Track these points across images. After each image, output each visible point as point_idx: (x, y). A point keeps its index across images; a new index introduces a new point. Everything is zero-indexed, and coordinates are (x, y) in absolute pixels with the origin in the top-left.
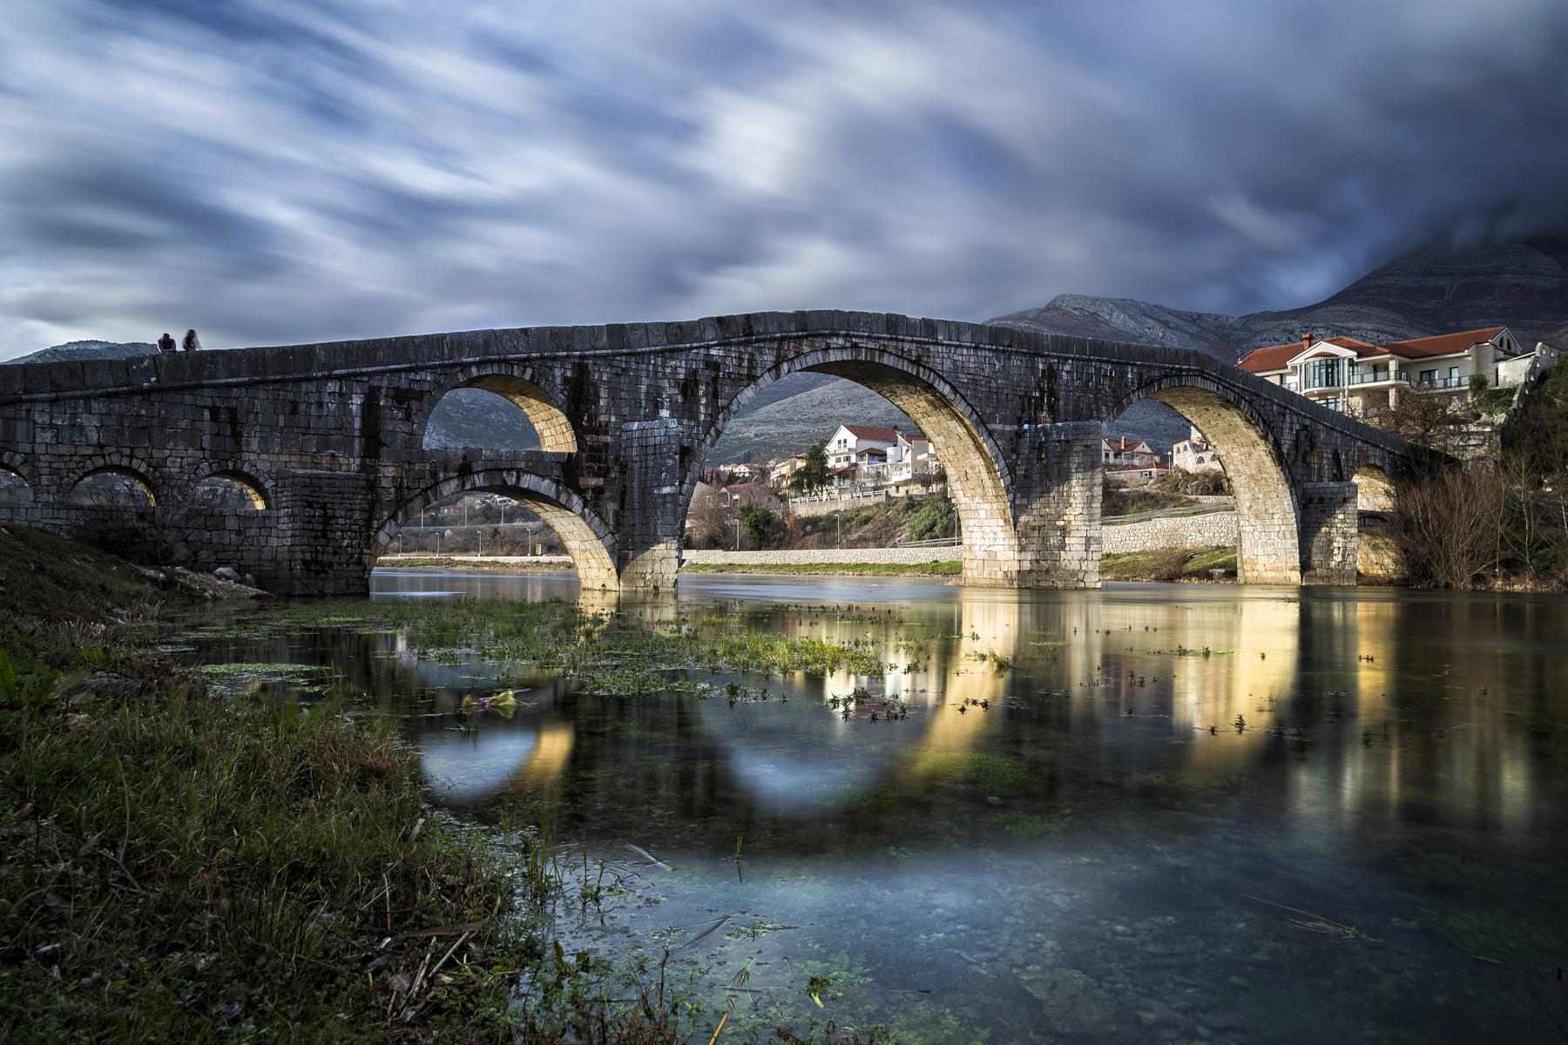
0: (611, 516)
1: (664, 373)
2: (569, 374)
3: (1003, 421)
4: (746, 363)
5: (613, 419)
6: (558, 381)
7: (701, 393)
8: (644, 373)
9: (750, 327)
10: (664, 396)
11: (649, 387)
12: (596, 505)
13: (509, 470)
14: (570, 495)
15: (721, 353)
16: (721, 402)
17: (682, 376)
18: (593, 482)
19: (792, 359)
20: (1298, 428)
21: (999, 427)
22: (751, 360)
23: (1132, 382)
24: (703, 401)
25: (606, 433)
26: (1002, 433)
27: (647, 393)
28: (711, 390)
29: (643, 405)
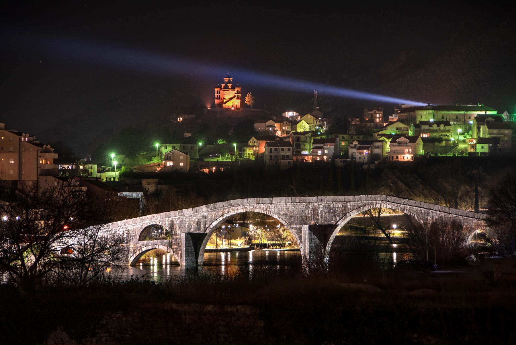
0: (179, 254)
1: (192, 220)
2: (169, 223)
3: (296, 224)
4: (213, 216)
5: (180, 232)
6: (167, 224)
7: (201, 224)
8: (187, 221)
9: (215, 207)
10: (192, 226)
11: (188, 224)
12: (176, 252)
13: (157, 245)
14: (170, 250)
15: (207, 214)
16: (207, 226)
17: (197, 221)
18: (175, 247)
19: (227, 213)
20: (437, 217)
21: (294, 226)
22: (215, 215)
23: (351, 209)
24: (202, 226)
25: (178, 236)
26: (296, 228)
27: (188, 225)
28: (204, 223)
29: (187, 228)
